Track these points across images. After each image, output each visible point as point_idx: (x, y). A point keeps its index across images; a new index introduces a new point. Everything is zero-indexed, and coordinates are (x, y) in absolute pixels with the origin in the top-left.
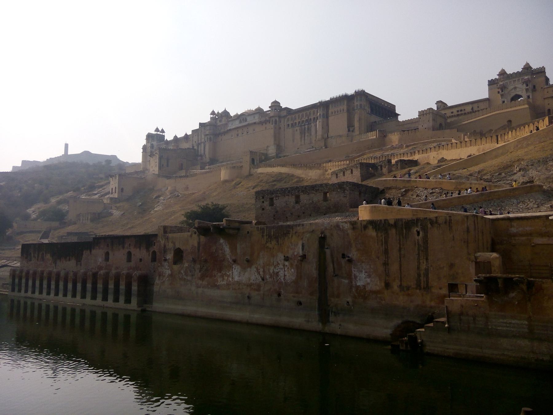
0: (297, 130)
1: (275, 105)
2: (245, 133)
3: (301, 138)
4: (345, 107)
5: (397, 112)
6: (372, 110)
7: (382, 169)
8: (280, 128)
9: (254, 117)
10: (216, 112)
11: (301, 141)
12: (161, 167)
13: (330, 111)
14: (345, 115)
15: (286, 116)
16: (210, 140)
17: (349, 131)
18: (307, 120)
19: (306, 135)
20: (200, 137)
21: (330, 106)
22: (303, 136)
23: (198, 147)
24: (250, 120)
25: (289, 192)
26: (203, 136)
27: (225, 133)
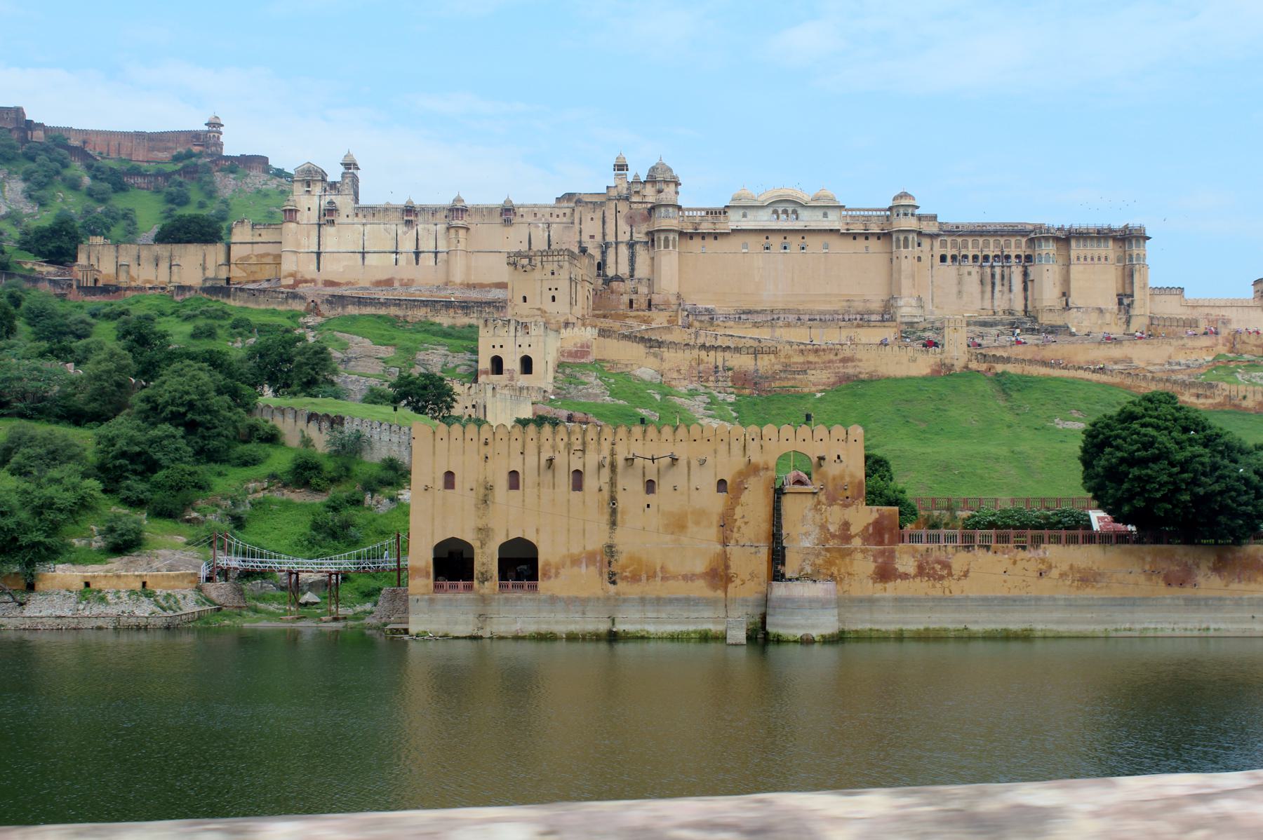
0: (969, 273)
1: (903, 206)
3: (983, 292)
8: (919, 259)
9: (825, 215)
11: (982, 298)
13: (1073, 254)
16: (674, 246)
17: (1120, 303)
19: (998, 287)
21: (1073, 243)
22: (989, 288)
23: (604, 253)
24: (809, 219)
26: (624, 226)
27: (716, 236)
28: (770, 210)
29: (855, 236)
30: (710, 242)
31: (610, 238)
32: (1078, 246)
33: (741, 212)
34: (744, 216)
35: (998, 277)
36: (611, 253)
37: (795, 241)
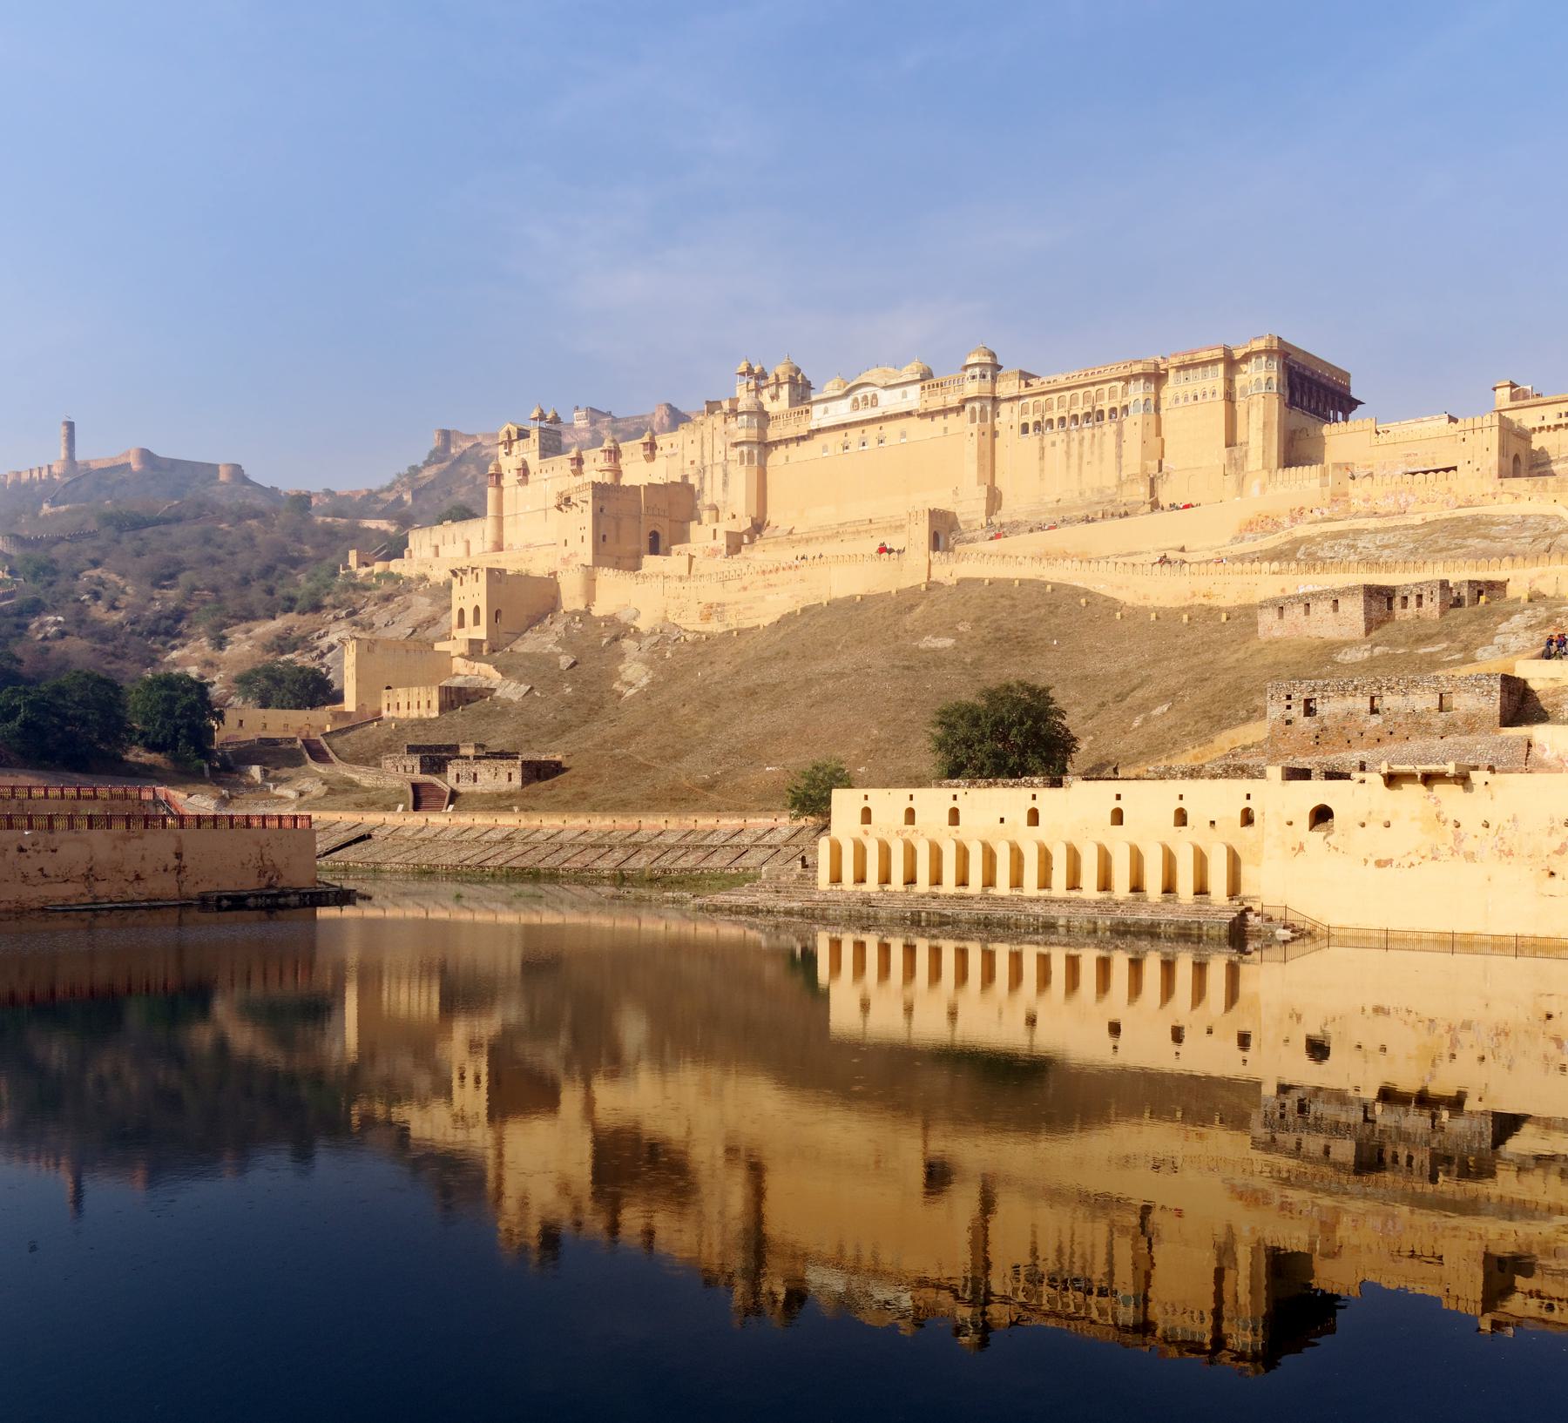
0: (1053, 444)
2: (872, 444)
3: (1068, 467)
4: (1220, 386)
5: (1355, 394)
6: (1292, 395)
7: (1419, 604)
8: (995, 434)
9: (904, 395)
10: (757, 369)
12: (600, 540)
14: (1221, 407)
15: (1019, 398)
16: (750, 460)
18: (1088, 415)
20: (707, 447)
23: (702, 480)
24: (890, 401)
25: (1356, 688)
26: (719, 446)
27: (799, 439)
28: (850, 400)
29: (931, 415)
30: (793, 446)
31: (707, 462)
32: (1177, 381)
33: (822, 406)
34: (826, 411)
35: (1087, 443)
36: (708, 475)
37: (872, 430)
